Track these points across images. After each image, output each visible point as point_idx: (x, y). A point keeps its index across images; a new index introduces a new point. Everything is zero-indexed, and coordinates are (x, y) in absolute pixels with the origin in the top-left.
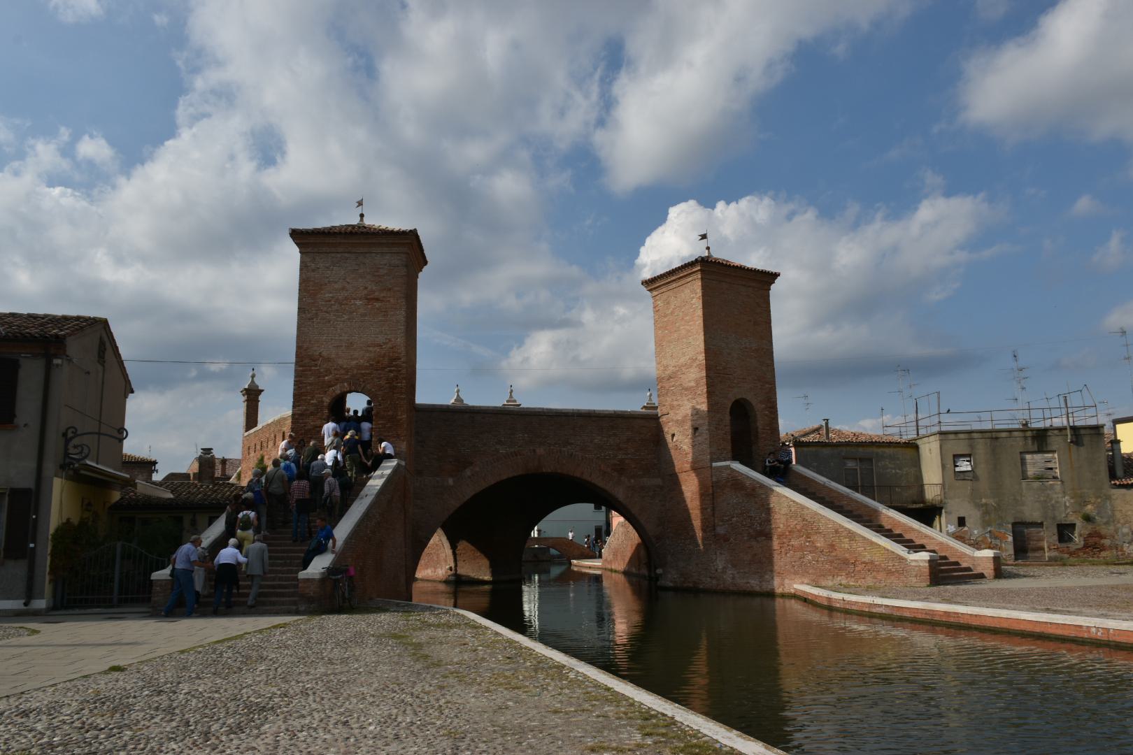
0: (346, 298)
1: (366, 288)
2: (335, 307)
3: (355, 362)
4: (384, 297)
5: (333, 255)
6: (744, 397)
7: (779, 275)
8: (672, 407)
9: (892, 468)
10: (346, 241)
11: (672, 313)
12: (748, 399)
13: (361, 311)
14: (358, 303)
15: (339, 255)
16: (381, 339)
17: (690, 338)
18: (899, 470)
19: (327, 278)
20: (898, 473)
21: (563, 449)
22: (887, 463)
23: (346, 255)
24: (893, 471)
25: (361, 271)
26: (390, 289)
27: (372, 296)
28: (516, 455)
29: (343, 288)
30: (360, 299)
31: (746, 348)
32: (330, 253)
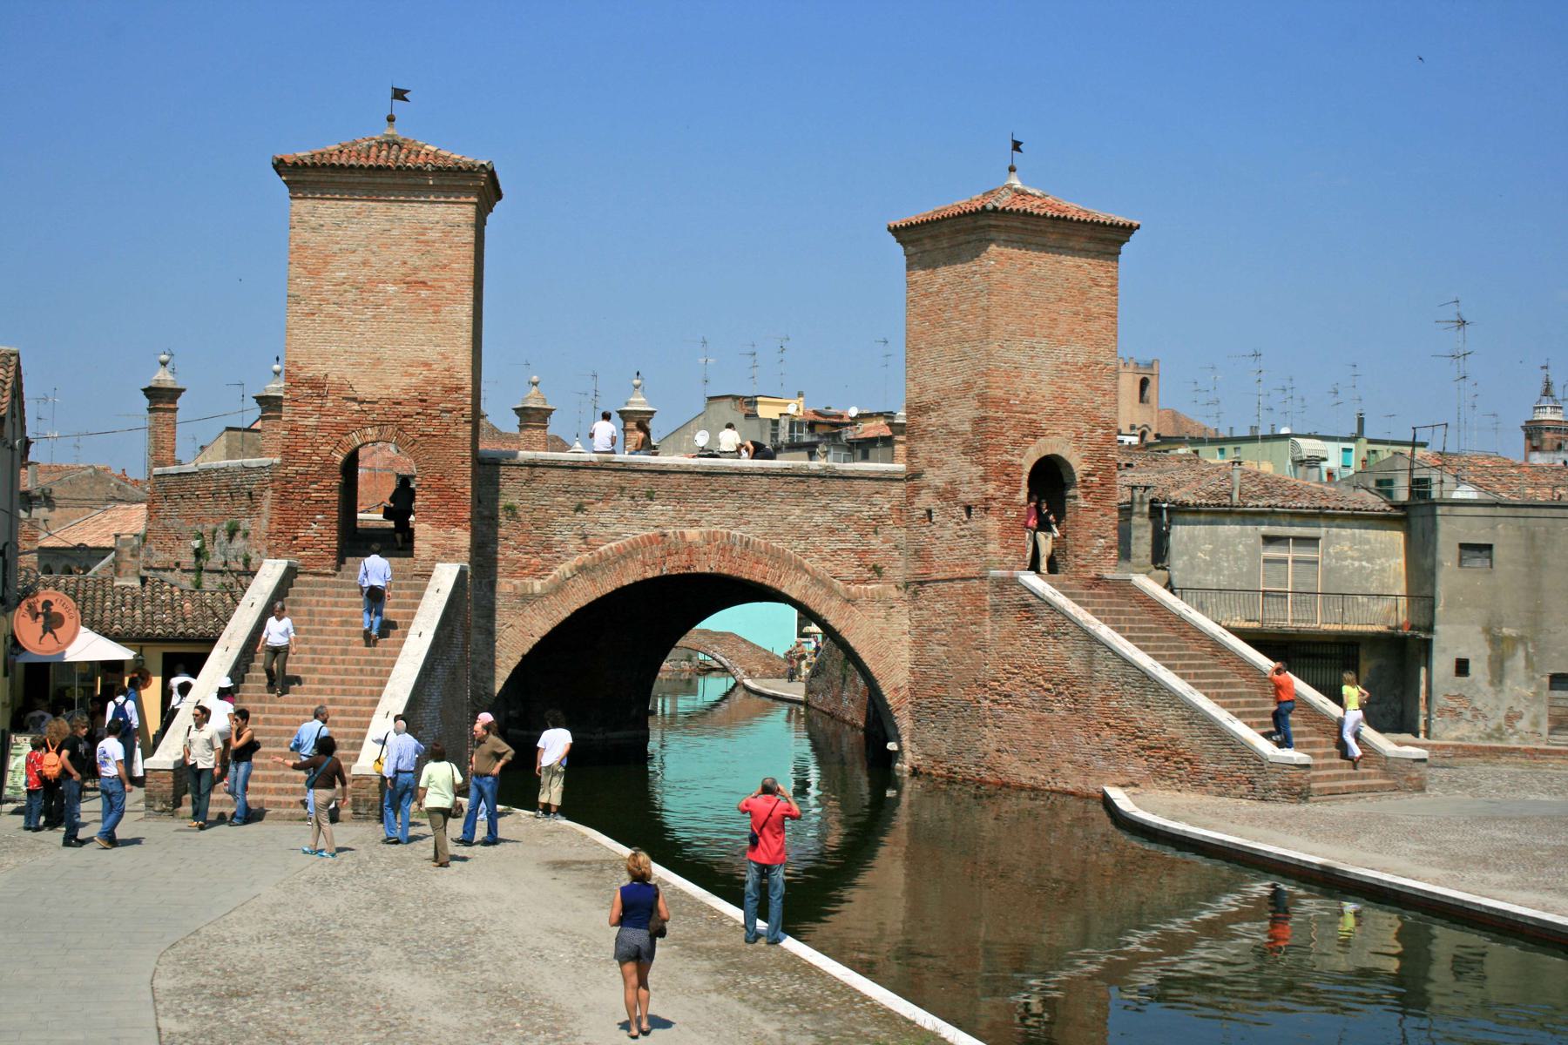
0: (370, 280)
2: (350, 296)
3: (386, 392)
4: (435, 280)
5: (347, 203)
6: (1056, 451)
7: (1138, 227)
8: (931, 464)
9: (1353, 558)
10: (370, 180)
11: (939, 292)
12: (1063, 456)
13: (396, 303)
14: (391, 288)
16: (430, 353)
17: (967, 345)
18: (1368, 562)
19: (338, 243)
20: (1364, 568)
21: (733, 532)
22: (1346, 548)
23: (370, 203)
24: (1357, 564)
25: (394, 232)
26: (445, 266)
27: (413, 278)
28: (652, 543)
30: (395, 283)
31: (1067, 363)
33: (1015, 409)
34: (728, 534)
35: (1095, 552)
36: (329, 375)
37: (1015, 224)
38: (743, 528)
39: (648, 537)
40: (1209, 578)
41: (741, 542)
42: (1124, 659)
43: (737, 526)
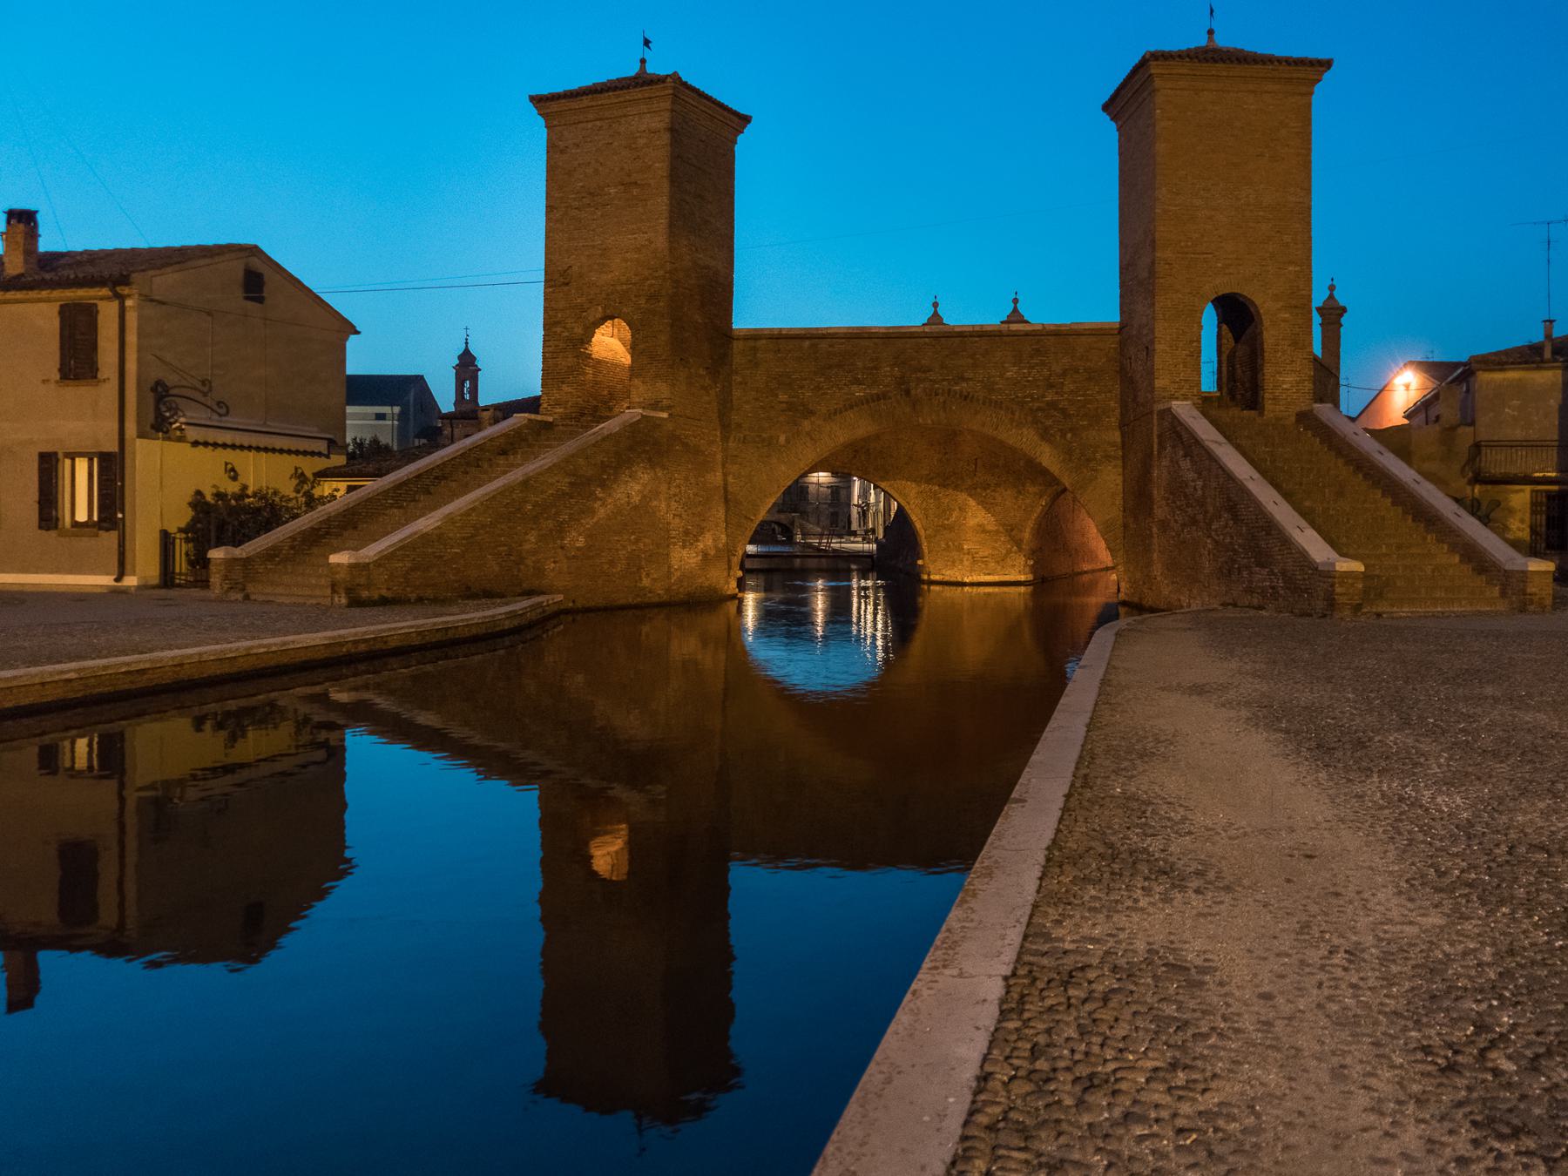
1: (622, 169)
7: (1327, 64)
14: (612, 191)
15: (590, 125)
19: (576, 160)
23: (598, 123)
29: (596, 171)
30: (616, 186)
32: (579, 122)
33: (1186, 250)
34: (949, 390)
35: (1285, 386)
36: (575, 268)
37: (1180, 71)
38: (964, 385)
39: (878, 395)
40: (1518, 432)
41: (961, 396)
42: (1228, 475)
43: (956, 384)
